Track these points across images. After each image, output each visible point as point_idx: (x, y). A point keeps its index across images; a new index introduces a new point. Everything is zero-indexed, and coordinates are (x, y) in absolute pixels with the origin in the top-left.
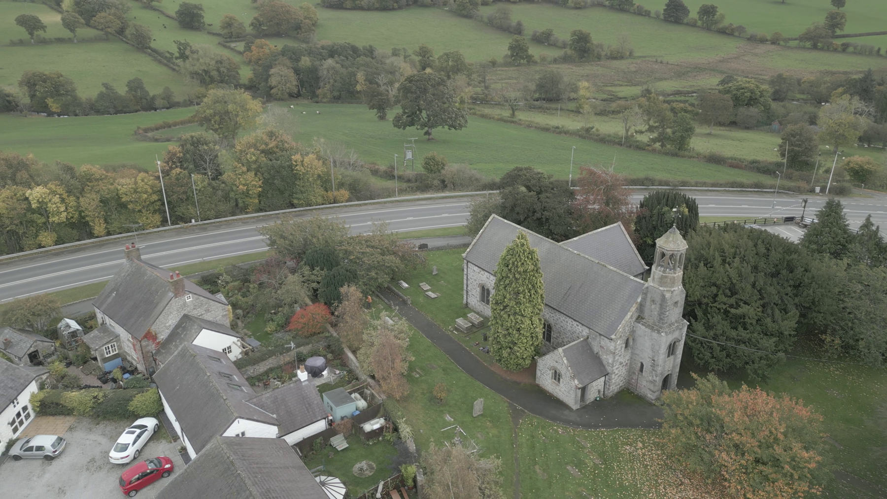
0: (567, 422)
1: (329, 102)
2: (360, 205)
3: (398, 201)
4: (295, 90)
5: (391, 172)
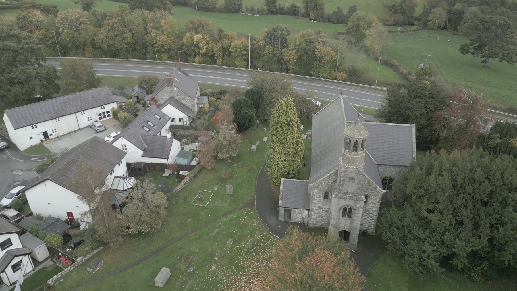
0: (266, 224)
1: (462, 35)
2: (349, 85)
3: (375, 89)
4: (443, 24)
5: (407, 75)
